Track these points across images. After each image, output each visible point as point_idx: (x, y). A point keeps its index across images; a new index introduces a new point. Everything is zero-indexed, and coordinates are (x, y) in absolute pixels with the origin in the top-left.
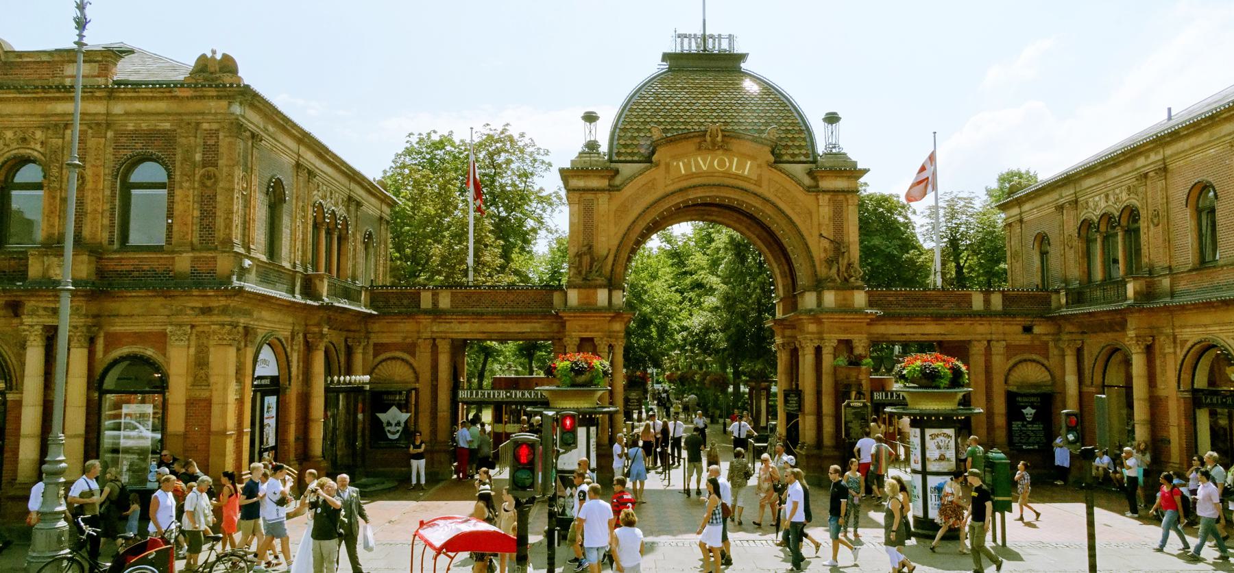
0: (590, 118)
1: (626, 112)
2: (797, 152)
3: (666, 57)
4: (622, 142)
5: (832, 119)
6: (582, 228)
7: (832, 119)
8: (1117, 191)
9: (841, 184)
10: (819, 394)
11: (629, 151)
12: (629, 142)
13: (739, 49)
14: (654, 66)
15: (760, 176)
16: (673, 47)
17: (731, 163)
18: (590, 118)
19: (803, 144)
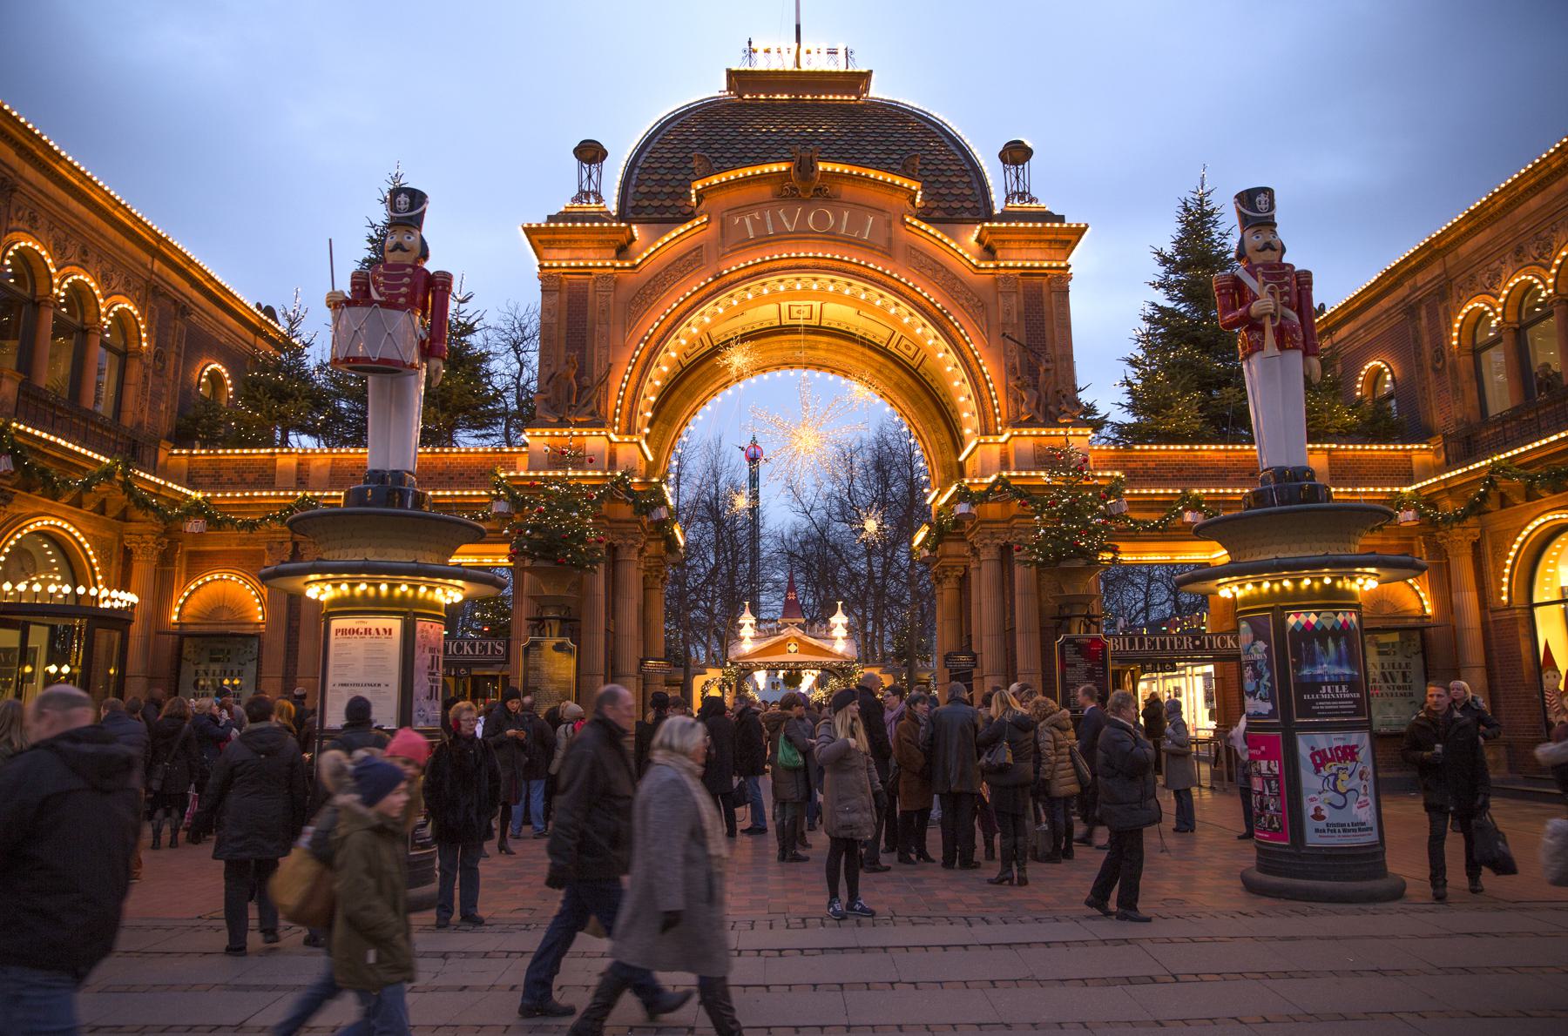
0: (590, 153)
1: (653, 144)
2: (956, 205)
3: (736, 78)
4: (643, 189)
5: (1016, 154)
6: (563, 333)
7: (1016, 154)
8: (1544, 234)
9: (1037, 259)
10: (1007, 635)
11: (656, 203)
12: (656, 189)
13: (860, 67)
14: (715, 87)
15: (890, 240)
16: (739, 65)
17: (838, 219)
18: (590, 153)
19: (967, 192)
